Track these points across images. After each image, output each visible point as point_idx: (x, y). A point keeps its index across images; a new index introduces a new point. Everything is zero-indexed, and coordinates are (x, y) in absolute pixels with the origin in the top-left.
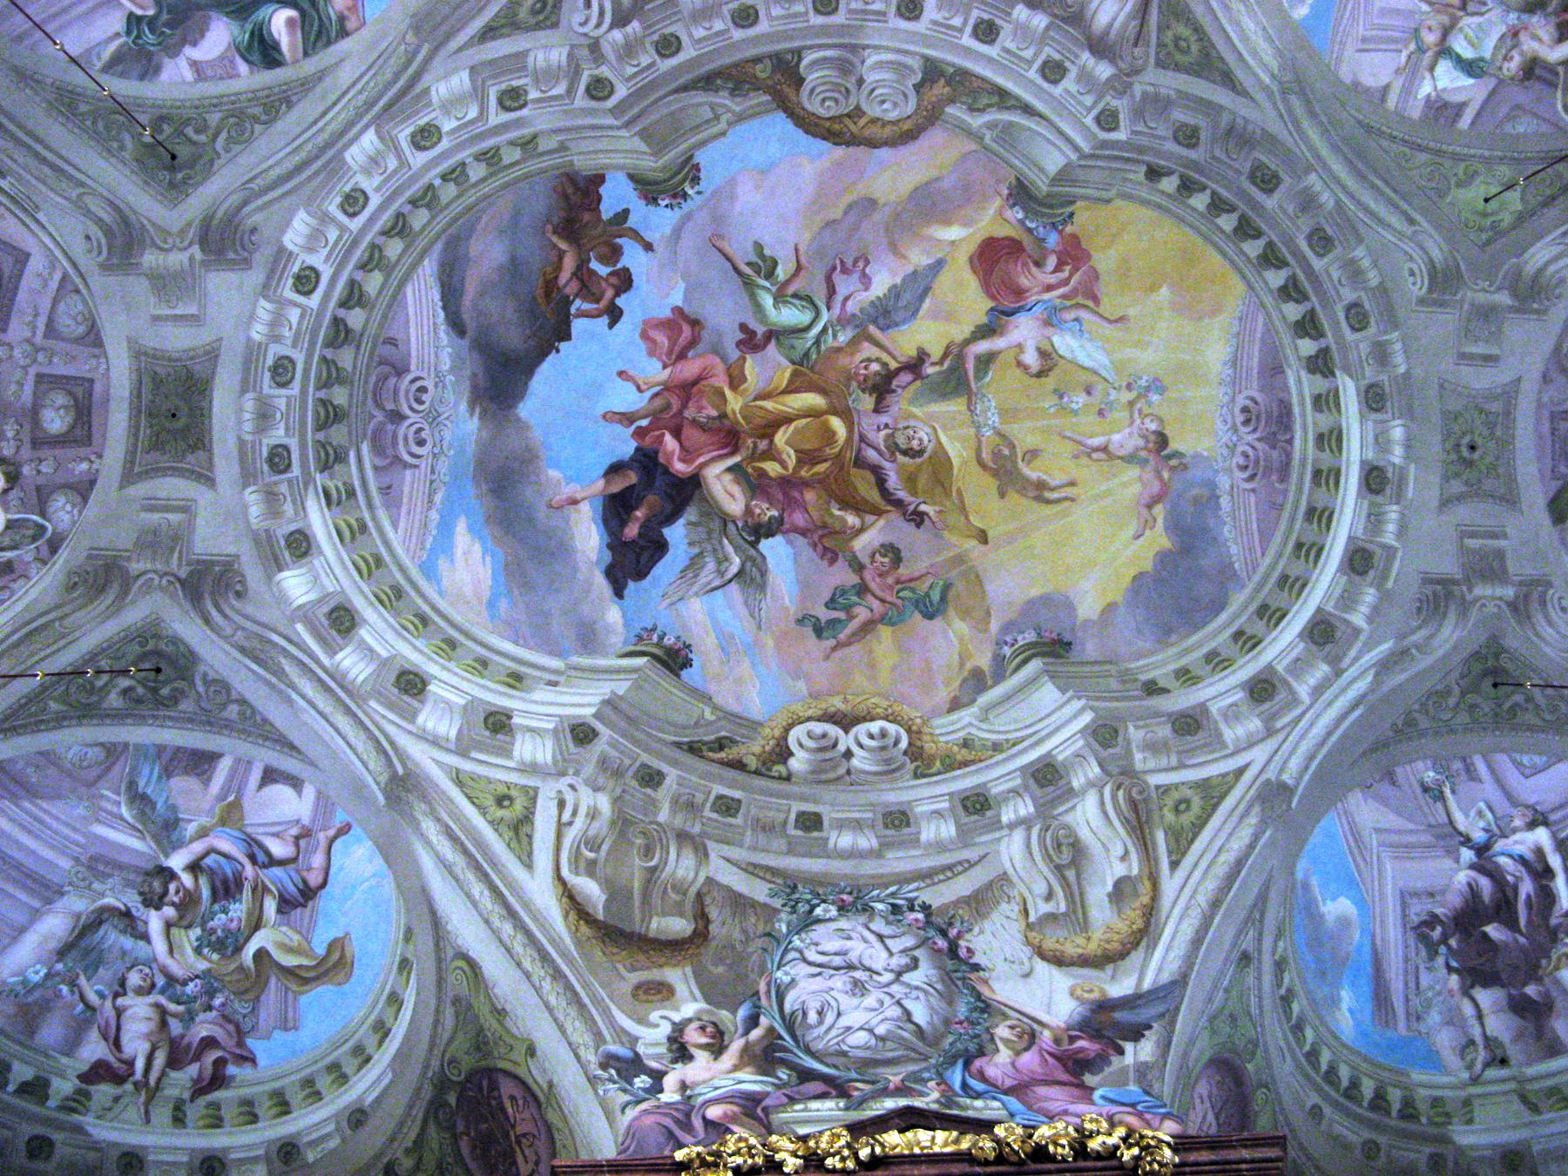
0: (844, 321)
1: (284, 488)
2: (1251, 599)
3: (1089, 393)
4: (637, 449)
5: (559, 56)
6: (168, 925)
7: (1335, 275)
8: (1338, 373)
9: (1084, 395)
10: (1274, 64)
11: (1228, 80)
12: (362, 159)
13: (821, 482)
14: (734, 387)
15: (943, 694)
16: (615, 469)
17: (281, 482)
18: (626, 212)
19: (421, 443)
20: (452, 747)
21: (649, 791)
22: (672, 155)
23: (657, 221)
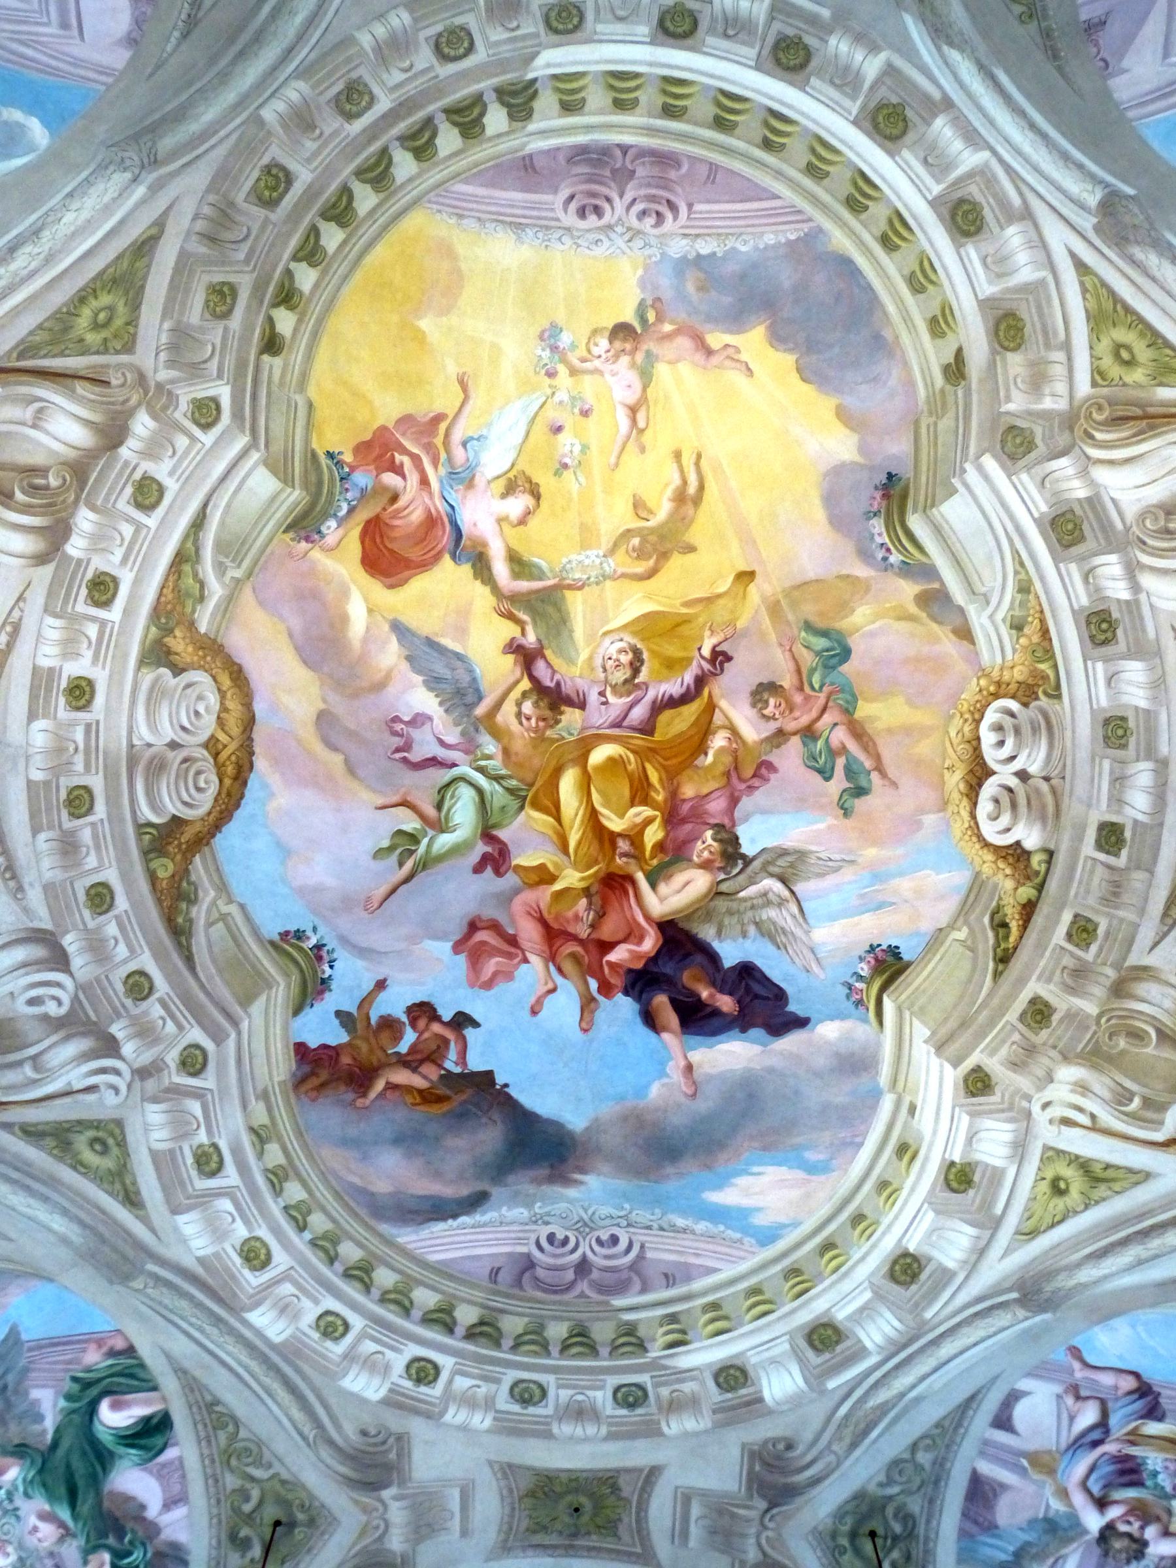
0: (469, 747)
1: (665, 1392)
2: (844, 225)
3: (559, 429)
4: (626, 993)
5: (155, 1114)
6: (1166, 1533)
7: (397, 77)
8: (530, 76)
9: (561, 437)
10: (120, 178)
11: (145, 248)
12: (281, 1325)
13: (672, 777)
14: (552, 879)
15: (949, 646)
17: (658, 1397)
18: (338, 1014)
19: (614, 1240)
20: (987, 1233)
21: (1055, 1018)
22: (268, 963)
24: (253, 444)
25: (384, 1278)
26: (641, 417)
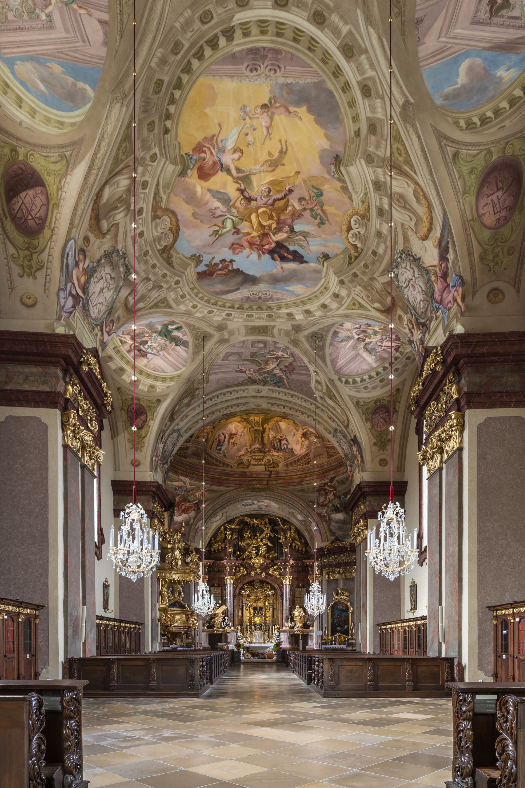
0: (229, 211)
9: (248, 136)
14: (250, 234)
16: (273, 259)
23: (206, 259)
24: (167, 159)
25: (220, 303)
26: (270, 130)
